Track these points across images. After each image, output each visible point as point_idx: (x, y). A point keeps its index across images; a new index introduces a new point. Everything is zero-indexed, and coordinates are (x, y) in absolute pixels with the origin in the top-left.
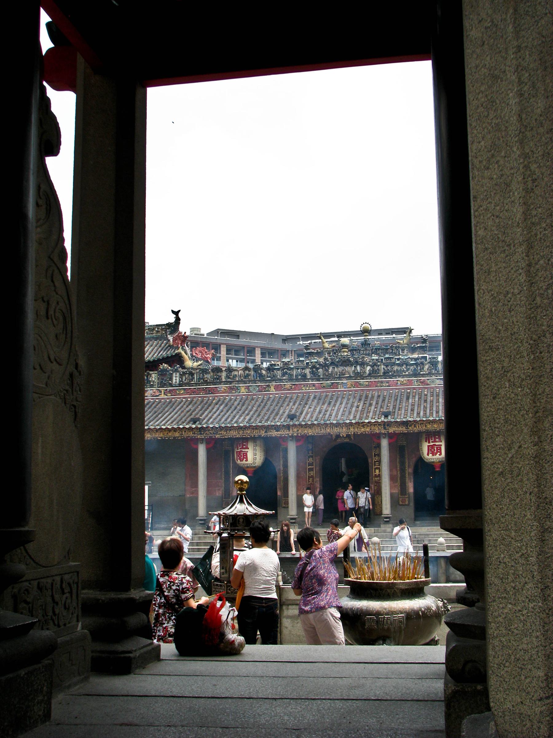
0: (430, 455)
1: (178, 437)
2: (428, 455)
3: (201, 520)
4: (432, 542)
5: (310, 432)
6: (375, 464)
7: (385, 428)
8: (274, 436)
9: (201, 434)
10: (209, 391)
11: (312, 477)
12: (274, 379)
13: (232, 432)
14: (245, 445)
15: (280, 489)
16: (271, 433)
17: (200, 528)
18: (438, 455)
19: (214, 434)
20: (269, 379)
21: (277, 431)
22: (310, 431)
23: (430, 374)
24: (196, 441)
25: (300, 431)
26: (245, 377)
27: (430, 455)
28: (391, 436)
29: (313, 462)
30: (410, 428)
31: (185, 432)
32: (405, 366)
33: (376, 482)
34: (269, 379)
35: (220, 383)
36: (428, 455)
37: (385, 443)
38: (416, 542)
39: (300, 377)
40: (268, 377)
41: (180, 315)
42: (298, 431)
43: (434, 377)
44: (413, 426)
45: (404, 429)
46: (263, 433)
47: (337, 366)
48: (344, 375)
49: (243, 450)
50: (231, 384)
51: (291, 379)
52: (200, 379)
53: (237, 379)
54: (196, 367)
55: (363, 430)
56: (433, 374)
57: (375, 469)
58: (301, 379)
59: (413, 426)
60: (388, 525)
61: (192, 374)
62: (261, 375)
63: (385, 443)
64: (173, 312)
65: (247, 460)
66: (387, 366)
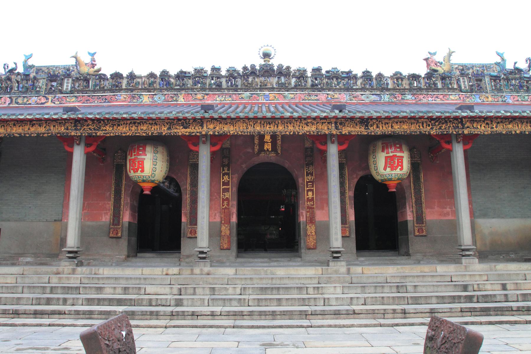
0: (388, 169)
1: (43, 134)
2: (385, 169)
3: (70, 252)
4: (419, 289)
5: (230, 129)
6: (307, 185)
7: (337, 128)
8: (180, 134)
10: (106, 99)
11: (227, 199)
12: (183, 88)
13: (120, 128)
14: (141, 150)
15: (186, 215)
16: (176, 131)
17: (67, 263)
18: (398, 170)
19: (94, 129)
20: (178, 87)
21: (185, 128)
22: (232, 128)
23: (363, 89)
24: (70, 141)
25: (217, 128)
26: (150, 84)
27: (388, 169)
28: (341, 139)
29: (229, 181)
30: (371, 128)
31: (54, 126)
32: (335, 79)
33: (308, 207)
34: (178, 87)
35: (120, 90)
36: (385, 169)
37: (333, 151)
38: (394, 290)
39: (214, 87)
40: (176, 86)
41: (95, 57)
42: (214, 128)
43: (368, 92)
44: (375, 126)
45: (363, 129)
46: (164, 130)
48: (266, 85)
49: (139, 157)
50: (132, 91)
51: (203, 89)
52: (96, 85)
53: (140, 87)
54: (92, 73)
55: (306, 129)
56: (367, 89)
57: (308, 191)
58: (215, 89)
59: (375, 126)
60: (339, 263)
61: (87, 80)
62: (168, 83)
63: (333, 151)
64: (89, 53)
65: (142, 171)
66: (316, 79)
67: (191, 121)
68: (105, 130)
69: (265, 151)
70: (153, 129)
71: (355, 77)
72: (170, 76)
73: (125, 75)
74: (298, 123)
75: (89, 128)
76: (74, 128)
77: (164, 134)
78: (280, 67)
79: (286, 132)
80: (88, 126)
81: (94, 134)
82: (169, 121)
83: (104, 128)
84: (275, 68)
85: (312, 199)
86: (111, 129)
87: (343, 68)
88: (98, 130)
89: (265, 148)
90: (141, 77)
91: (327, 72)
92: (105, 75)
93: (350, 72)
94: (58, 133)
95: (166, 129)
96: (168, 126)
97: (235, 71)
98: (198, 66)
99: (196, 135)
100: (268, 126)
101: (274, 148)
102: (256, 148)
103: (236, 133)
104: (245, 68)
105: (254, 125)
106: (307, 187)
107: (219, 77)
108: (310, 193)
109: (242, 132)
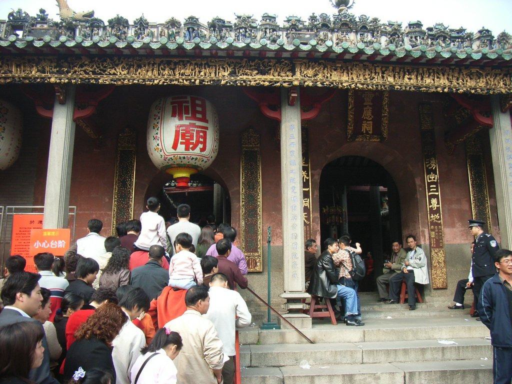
6: (429, 188)
8: (253, 83)
9: (59, 72)
16: (245, 77)
19: (94, 73)
21: (263, 73)
22: (345, 78)
25: (320, 77)
33: (433, 223)
42: (315, 75)
47: (332, 31)
55: (469, 84)
57: (431, 197)
67: (274, 61)
68: (114, 74)
69: (362, 133)
70: (202, 73)
71: (469, 37)
72: (199, 26)
73: (131, 23)
74: (456, 75)
75: (85, 71)
76: (55, 70)
77: (223, 82)
78: (363, 19)
79: (436, 88)
80: (81, 66)
81: (93, 81)
82: (232, 60)
83: (113, 71)
84: (357, 20)
85: (437, 211)
86: (125, 72)
87: (453, 24)
88: (100, 74)
89: (363, 130)
90: (156, 26)
91: (430, 29)
92: (101, 21)
93: (461, 31)
94: (24, 78)
95: (226, 74)
96: (230, 70)
97: (299, 21)
98: (244, 13)
99: (281, 87)
100: (407, 76)
101: (377, 131)
102: (350, 129)
103: (353, 86)
104: (313, 18)
105: (383, 73)
106: (429, 191)
107: (275, 29)
108: (434, 201)
109: (363, 84)
